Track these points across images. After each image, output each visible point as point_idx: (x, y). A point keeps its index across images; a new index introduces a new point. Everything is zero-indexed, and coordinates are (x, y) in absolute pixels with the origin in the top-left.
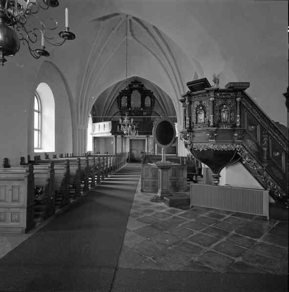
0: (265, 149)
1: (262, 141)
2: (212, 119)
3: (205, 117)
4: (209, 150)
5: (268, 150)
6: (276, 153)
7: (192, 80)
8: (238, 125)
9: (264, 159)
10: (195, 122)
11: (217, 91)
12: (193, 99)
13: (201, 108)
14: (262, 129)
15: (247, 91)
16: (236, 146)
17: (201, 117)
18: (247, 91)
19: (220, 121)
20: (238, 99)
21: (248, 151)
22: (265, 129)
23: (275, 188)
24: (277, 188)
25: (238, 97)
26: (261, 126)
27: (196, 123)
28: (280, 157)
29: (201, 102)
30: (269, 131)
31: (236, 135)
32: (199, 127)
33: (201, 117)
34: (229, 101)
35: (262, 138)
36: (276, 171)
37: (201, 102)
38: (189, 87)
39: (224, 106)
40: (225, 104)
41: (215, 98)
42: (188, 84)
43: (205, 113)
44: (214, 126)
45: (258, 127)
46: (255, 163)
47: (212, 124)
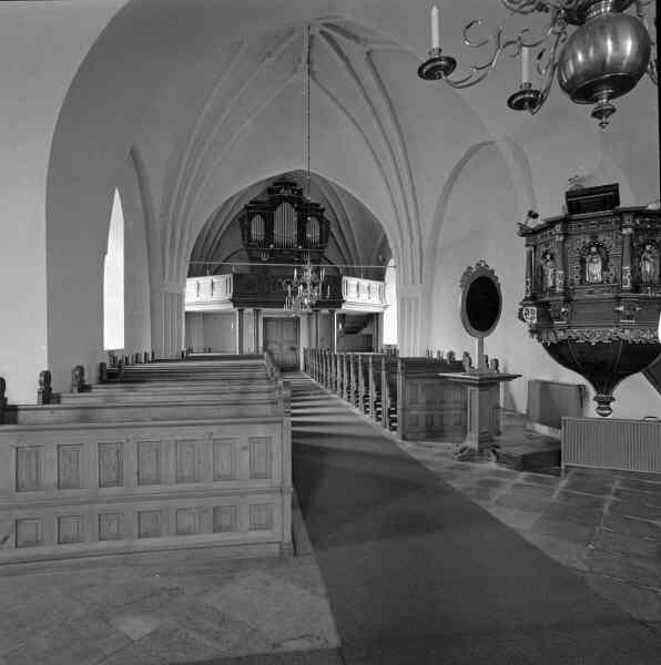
3: (605, 268)
10: (577, 281)
12: (573, 228)
13: (594, 249)
17: (595, 270)
29: (594, 237)
32: (591, 292)
33: (595, 270)
37: (594, 237)
39: (648, 248)
40: (648, 243)
44: (632, 291)
47: (628, 286)
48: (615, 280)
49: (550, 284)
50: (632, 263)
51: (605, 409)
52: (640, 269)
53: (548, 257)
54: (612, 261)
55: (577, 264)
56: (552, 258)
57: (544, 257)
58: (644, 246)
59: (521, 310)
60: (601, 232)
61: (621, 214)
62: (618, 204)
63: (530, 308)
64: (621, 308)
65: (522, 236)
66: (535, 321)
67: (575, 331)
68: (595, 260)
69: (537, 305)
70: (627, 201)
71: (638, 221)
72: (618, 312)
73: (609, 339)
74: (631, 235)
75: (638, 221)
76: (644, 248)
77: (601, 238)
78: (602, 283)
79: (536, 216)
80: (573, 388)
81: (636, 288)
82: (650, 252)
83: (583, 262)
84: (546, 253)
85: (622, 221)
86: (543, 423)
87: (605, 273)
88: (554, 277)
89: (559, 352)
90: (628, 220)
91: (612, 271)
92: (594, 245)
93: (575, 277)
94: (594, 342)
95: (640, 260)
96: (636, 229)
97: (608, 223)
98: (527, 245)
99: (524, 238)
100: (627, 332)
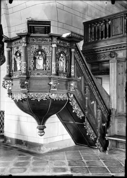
1: (85, 92)
3: (45, 63)
4: (48, 100)
5: (88, 99)
6: (92, 102)
8: (72, 75)
10: (32, 68)
13: (40, 53)
17: (40, 63)
23: (91, 132)
24: (92, 132)
25: (73, 48)
26: (85, 78)
29: (40, 47)
32: (38, 74)
33: (40, 63)
37: (40, 47)
39: (62, 55)
40: (61, 53)
43: (45, 60)
48: (49, 69)
53: (18, 54)
54: (47, 59)
58: (60, 54)
60: (44, 44)
61: (52, 37)
68: (40, 58)
71: (58, 41)
75: (58, 41)
76: (60, 56)
78: (43, 69)
82: (62, 57)
83: (35, 58)
87: (44, 65)
90: (55, 40)
91: (47, 64)
92: (40, 51)
93: (31, 66)
97: (46, 40)
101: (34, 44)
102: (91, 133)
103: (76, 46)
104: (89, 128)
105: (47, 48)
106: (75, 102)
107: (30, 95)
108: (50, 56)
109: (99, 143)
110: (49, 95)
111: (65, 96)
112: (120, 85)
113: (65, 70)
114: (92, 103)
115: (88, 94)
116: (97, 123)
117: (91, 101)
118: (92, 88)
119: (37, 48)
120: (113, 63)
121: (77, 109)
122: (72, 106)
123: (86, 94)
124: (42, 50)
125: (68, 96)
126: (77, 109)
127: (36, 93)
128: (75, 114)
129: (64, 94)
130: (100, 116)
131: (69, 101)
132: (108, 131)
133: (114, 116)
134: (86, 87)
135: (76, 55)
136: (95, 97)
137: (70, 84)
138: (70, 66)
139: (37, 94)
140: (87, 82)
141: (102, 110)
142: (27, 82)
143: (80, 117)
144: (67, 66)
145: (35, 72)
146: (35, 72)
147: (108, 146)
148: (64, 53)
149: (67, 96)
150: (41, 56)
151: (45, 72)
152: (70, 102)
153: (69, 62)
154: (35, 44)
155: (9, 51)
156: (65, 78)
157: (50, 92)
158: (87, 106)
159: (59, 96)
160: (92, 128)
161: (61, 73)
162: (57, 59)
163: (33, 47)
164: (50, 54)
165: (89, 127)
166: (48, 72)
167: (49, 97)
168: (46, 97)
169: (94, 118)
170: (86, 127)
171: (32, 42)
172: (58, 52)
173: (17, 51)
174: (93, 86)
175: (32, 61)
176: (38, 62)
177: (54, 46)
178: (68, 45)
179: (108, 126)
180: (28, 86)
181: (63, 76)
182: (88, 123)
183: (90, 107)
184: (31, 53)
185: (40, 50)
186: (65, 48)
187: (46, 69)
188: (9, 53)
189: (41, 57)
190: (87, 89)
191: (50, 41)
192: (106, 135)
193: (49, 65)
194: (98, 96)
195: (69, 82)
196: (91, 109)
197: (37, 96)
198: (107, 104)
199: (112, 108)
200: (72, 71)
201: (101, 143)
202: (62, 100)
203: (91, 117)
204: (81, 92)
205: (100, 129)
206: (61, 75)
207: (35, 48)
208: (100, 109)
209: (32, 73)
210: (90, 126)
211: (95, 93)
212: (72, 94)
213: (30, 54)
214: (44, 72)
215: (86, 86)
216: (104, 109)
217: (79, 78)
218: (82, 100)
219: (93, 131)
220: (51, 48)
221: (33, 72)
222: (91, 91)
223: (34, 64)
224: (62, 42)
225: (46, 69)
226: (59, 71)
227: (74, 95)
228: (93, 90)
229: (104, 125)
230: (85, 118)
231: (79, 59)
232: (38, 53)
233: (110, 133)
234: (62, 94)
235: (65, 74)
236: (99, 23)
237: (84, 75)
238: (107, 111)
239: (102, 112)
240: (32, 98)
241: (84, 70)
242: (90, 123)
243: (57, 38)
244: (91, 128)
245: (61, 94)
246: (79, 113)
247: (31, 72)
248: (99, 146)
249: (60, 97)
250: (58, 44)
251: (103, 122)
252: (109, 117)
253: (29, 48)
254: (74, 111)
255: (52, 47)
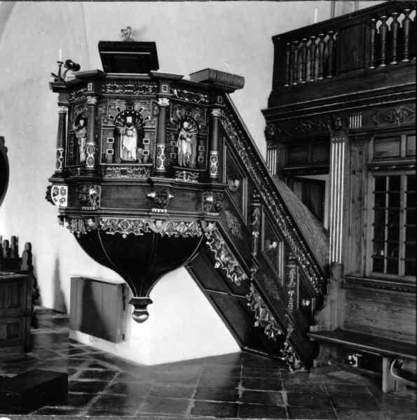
0: (255, 234)
1: (251, 219)
2: (163, 154)
3: (140, 145)
4: (150, 236)
5: (260, 236)
6: (271, 244)
7: (116, 37)
8: (214, 175)
9: (252, 256)
10: (109, 157)
11: (176, 82)
13: (129, 120)
14: (252, 185)
15: (236, 98)
16: (207, 226)
17: (129, 143)
18: (236, 98)
19: (175, 162)
20: (216, 112)
21: (225, 238)
22: (256, 188)
23: (267, 320)
24: (269, 319)
25: (217, 107)
26: (250, 181)
27: (114, 161)
28: (275, 251)
29: (130, 103)
30: (262, 194)
31: (210, 199)
32: (123, 172)
33: (129, 143)
34: (196, 115)
35: (251, 209)
36: (269, 283)
37: (130, 103)
38: (101, 55)
39: (186, 124)
41: (171, 101)
42: (104, 46)
43: (141, 135)
45: (245, 182)
46: (235, 267)
47: (161, 168)
48: (150, 160)
49: (82, 157)
50: (166, 142)
51: (142, 313)
52: (176, 149)
53: (82, 122)
54: (147, 135)
55: (110, 136)
56: (85, 124)
57: (77, 123)
58: (181, 121)
59: (49, 188)
60: (139, 99)
62: (157, 67)
63: (60, 187)
64: (153, 195)
65: (55, 90)
66: (65, 205)
67: (105, 219)
68: (130, 133)
69: (67, 183)
70: (166, 66)
71: (175, 91)
72: (151, 198)
73: (141, 231)
74: (167, 108)
75: (175, 91)
76: (182, 126)
77: (137, 107)
78: (137, 162)
79: (76, 67)
80: (115, 288)
81: (170, 172)
82: (187, 130)
83: (117, 134)
84: (80, 117)
85: (158, 90)
86: (84, 329)
87: (140, 150)
88: (87, 156)
89: (93, 244)
91: (147, 149)
92: (130, 115)
94: (125, 234)
95: (176, 140)
96: (173, 100)
97: (144, 88)
98: (60, 105)
99: (57, 94)
100: (159, 223)
101: (115, 99)
102: (267, 323)
103: (227, 102)
104: (261, 310)
105: (147, 109)
106: (223, 243)
107: (103, 222)
108: (154, 129)
109: (290, 348)
110: (147, 225)
111: (194, 226)
112: (353, 202)
113: (193, 162)
114: (271, 246)
115: (259, 222)
116: (285, 298)
117: (268, 241)
118: (274, 210)
119: (123, 107)
120: (338, 143)
121: (227, 259)
122: (214, 253)
123: (254, 223)
124: (135, 112)
125: (200, 226)
126: (227, 259)
127: (117, 219)
128: (221, 273)
129: (189, 223)
130: (295, 280)
131: (205, 239)
132: (317, 318)
133: (335, 280)
134: (253, 206)
135: (226, 125)
136: (280, 232)
137: (205, 198)
138: (209, 153)
139: (120, 221)
140: (258, 193)
141: (300, 266)
142: (94, 192)
143: (236, 279)
144: (201, 153)
145: (115, 167)
146: (115, 167)
147: (317, 354)
148: (193, 119)
149: (199, 227)
150: (131, 128)
151: (141, 167)
152: (208, 243)
153: (204, 140)
154: (118, 98)
155: (65, 114)
156: (194, 182)
157: (150, 216)
158: (255, 254)
159: (176, 227)
160: (268, 305)
161: (182, 170)
162: (172, 133)
163: (114, 105)
164: (152, 122)
165: (262, 307)
166: (146, 167)
167: (149, 229)
168: (143, 227)
169: (278, 285)
170: (253, 306)
171: (110, 93)
172: (177, 117)
173: (81, 115)
174: (277, 203)
175: (110, 140)
176: (124, 144)
177: (164, 102)
178: (203, 100)
179: (320, 305)
180: (99, 201)
181: (187, 178)
182: (260, 298)
183: (267, 258)
184: (108, 120)
185: (130, 112)
186: (195, 106)
187: (142, 160)
188: (65, 117)
189: (132, 130)
190: (256, 211)
191: (154, 90)
192: (312, 328)
193: (150, 149)
194: (290, 228)
195: (204, 193)
196: (270, 263)
197: (119, 226)
198: (317, 252)
199: (333, 261)
200: (215, 164)
201: (296, 349)
202: (184, 236)
203: (269, 283)
204: (240, 220)
205: (295, 313)
206: (183, 174)
207: (119, 109)
208: (296, 262)
209: (109, 169)
210: (265, 305)
211: (281, 221)
212: (212, 222)
213: (106, 123)
214: (137, 167)
215: (255, 204)
216: (308, 263)
217: (234, 182)
218: (240, 236)
219: (272, 318)
220: (156, 108)
221: (111, 167)
222: (270, 218)
223: (114, 148)
224: (186, 92)
225: (142, 160)
226: (178, 165)
227: (217, 225)
228: (275, 213)
229: (308, 303)
230: (252, 284)
231: (235, 134)
232: (126, 120)
233: (323, 323)
234: (185, 223)
235: (193, 172)
236: (393, 16)
237: (248, 175)
238: (318, 266)
239: (301, 271)
240: (108, 230)
241: (249, 161)
242: (263, 297)
243: (170, 82)
244: (268, 310)
245: (183, 223)
246: (232, 269)
247: (107, 167)
248: (290, 355)
249: (178, 229)
250: (174, 96)
251: (305, 292)
252: (324, 286)
253: (104, 107)
254: (217, 266)
255: (158, 105)
